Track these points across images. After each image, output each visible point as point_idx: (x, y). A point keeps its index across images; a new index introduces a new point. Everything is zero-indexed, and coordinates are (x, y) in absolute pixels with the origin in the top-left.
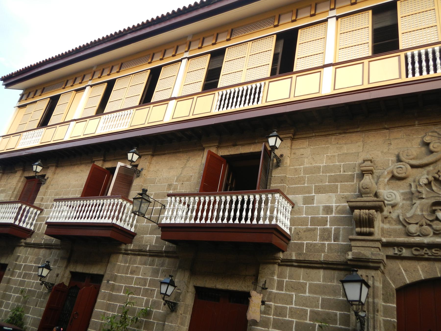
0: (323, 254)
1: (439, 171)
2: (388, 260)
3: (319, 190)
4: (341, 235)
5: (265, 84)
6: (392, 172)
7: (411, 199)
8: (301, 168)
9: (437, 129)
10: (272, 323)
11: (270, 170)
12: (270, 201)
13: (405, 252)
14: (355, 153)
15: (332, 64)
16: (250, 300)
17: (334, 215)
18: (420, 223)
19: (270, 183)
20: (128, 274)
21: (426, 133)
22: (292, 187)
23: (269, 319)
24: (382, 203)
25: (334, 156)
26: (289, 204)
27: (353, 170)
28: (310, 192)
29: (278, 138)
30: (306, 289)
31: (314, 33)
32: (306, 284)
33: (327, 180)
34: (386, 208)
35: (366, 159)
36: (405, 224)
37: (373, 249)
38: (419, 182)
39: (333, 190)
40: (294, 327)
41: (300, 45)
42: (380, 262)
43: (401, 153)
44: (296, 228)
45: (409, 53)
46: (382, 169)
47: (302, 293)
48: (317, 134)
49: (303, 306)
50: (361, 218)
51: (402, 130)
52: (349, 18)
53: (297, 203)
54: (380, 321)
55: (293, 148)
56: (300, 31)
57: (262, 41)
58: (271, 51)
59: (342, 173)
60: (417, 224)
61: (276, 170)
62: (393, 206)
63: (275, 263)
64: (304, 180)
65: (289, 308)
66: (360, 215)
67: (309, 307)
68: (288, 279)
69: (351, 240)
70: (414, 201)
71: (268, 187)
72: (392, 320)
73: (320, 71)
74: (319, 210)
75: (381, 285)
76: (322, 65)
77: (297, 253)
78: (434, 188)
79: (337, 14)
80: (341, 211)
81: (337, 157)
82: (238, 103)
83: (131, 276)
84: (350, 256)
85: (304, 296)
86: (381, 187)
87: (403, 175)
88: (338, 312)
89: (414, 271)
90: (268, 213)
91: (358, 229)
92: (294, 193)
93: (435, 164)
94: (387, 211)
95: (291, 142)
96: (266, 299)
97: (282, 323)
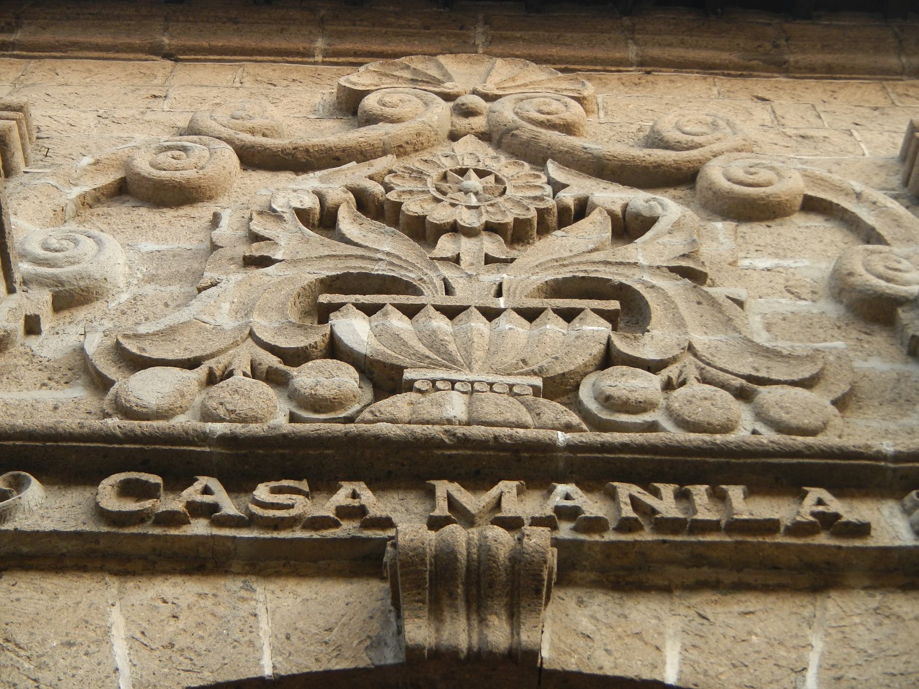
34: (14, 296)
36: (110, 370)
51: (241, 66)
60: (191, 364)
89: (70, 644)
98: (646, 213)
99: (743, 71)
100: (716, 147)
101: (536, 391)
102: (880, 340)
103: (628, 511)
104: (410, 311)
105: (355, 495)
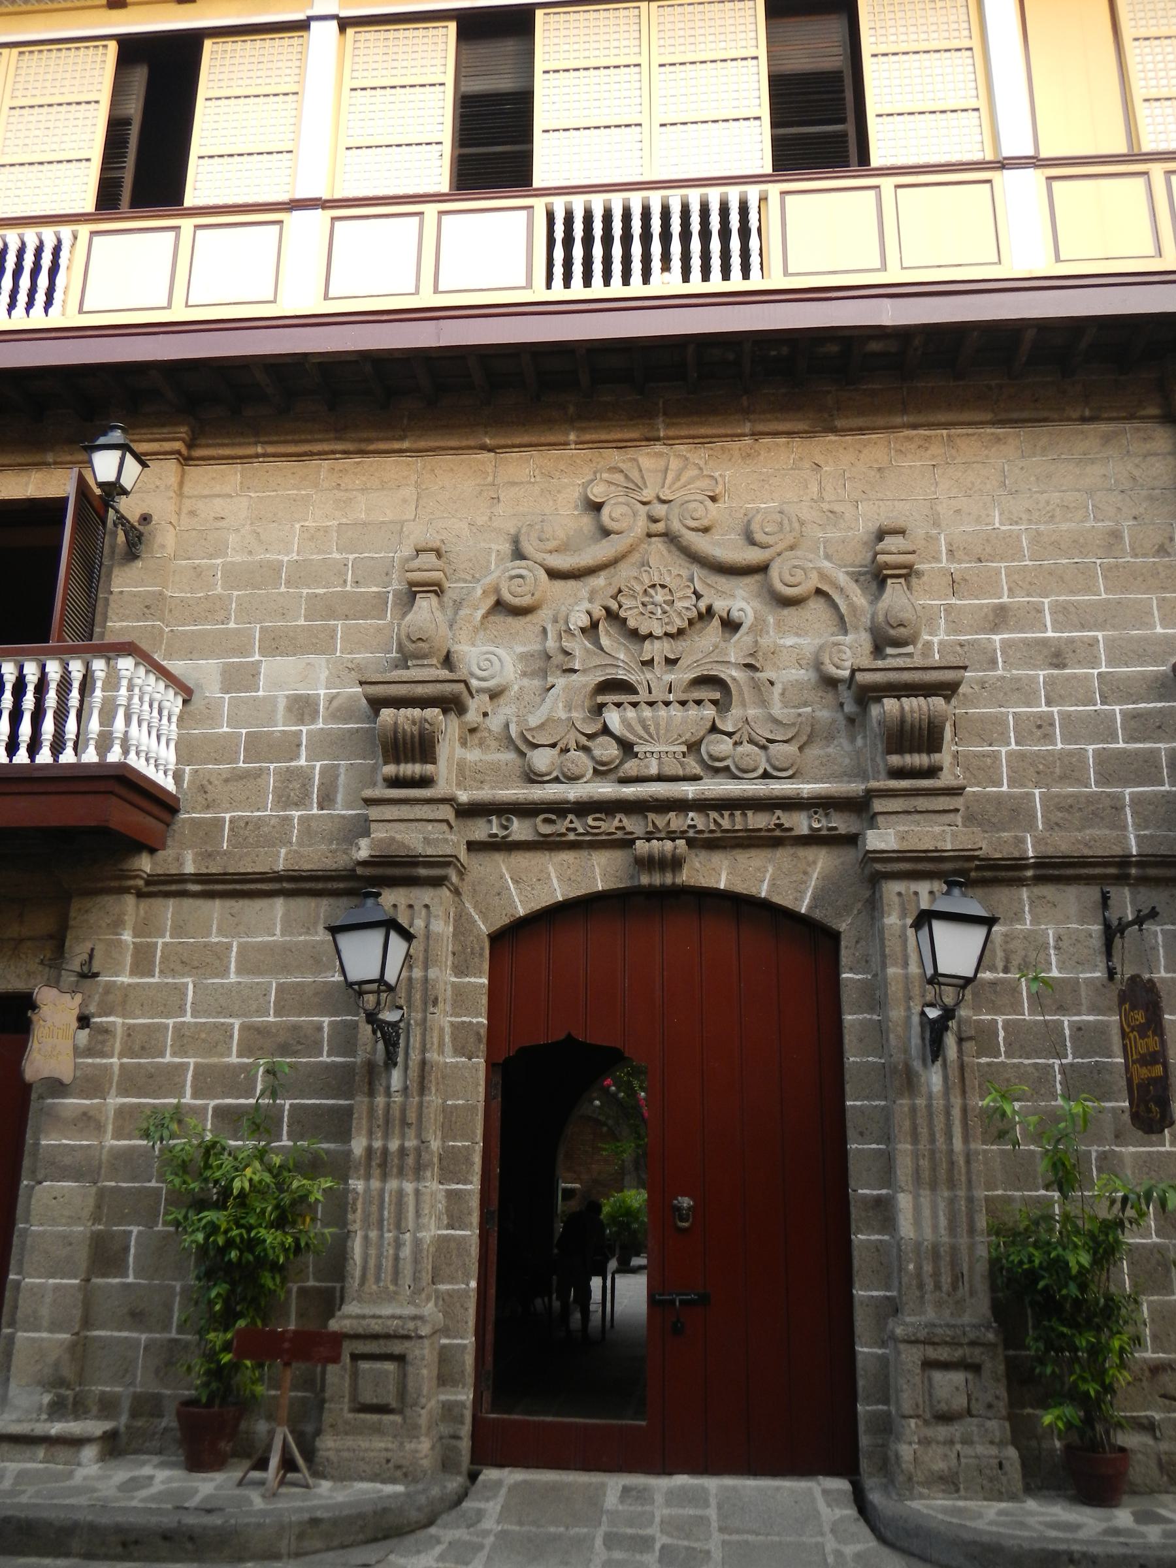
0: (283, 851)
1: (620, 591)
2: (473, 855)
3: (276, 644)
4: (341, 789)
5: (75, 238)
6: (497, 590)
7: (544, 673)
8: (215, 566)
9: (624, 461)
10: (116, 1079)
11: (103, 570)
12: (99, 684)
13: (520, 830)
14: (391, 522)
15: (319, 199)
16: (35, 1018)
17: (321, 725)
18: (560, 745)
19: (105, 618)
21: (595, 473)
22: (184, 633)
23: (107, 1068)
24: (462, 686)
25: (326, 530)
26: (171, 692)
27: (386, 579)
28: (244, 651)
29: (128, 456)
30: (230, 962)
31: (260, 66)
32: (228, 947)
33: (303, 611)
35: (422, 545)
36: (524, 748)
37: (430, 827)
38: (567, 623)
39: (320, 643)
40: (189, 1083)
41: (209, 103)
42: (447, 862)
43: (523, 531)
44: (197, 771)
45: (559, 205)
46: (469, 578)
47: (217, 976)
48: (270, 449)
49: (219, 1014)
50: (400, 736)
51: (531, 456)
52: (383, 35)
53: (200, 686)
54: (442, 1029)
55: (186, 494)
56: (208, 44)
57: (59, 54)
59: (348, 588)
60: (553, 746)
61: (126, 569)
62: (495, 695)
63: (126, 890)
64: (228, 610)
65: (174, 1027)
66: (396, 723)
67: (237, 1016)
68: (171, 937)
69: (370, 802)
70: (551, 680)
71: (97, 630)
72: (474, 1021)
73: (280, 222)
74: (274, 711)
75: (451, 929)
76: (284, 197)
77: (201, 854)
78: (605, 641)
79: (340, 7)
80: (341, 713)
81: (335, 534)
84: (363, 851)
85: (222, 985)
86: (463, 635)
87: (525, 601)
88: (326, 1020)
90: (94, 726)
91: (390, 769)
92: (190, 654)
93: (612, 570)
94: (477, 710)
95: (180, 468)
96: (92, 1009)
97: (151, 1076)
98: (737, 621)
99: (810, 433)
100: (778, 548)
101: (684, 753)
102: (830, 697)
103: (712, 827)
104: (635, 705)
105: (621, 821)
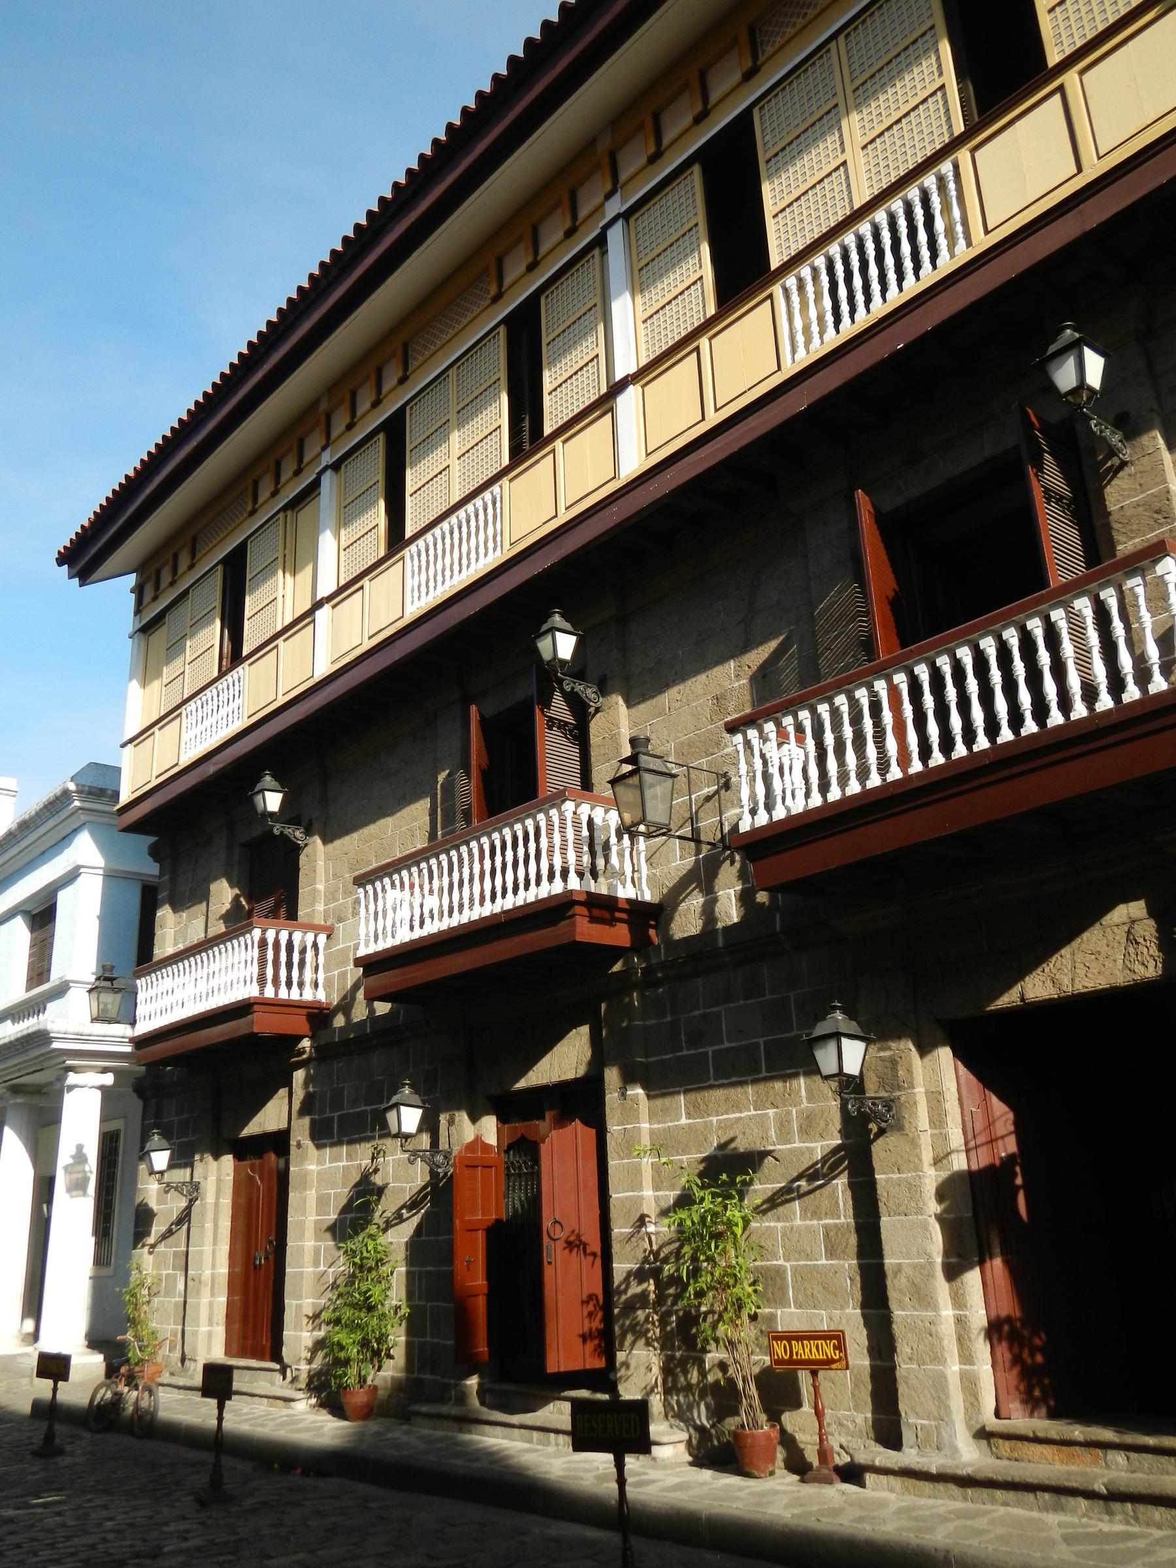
20: (681, 1050)
58: (933, 32)
82: (876, 287)
83: (693, 1052)
